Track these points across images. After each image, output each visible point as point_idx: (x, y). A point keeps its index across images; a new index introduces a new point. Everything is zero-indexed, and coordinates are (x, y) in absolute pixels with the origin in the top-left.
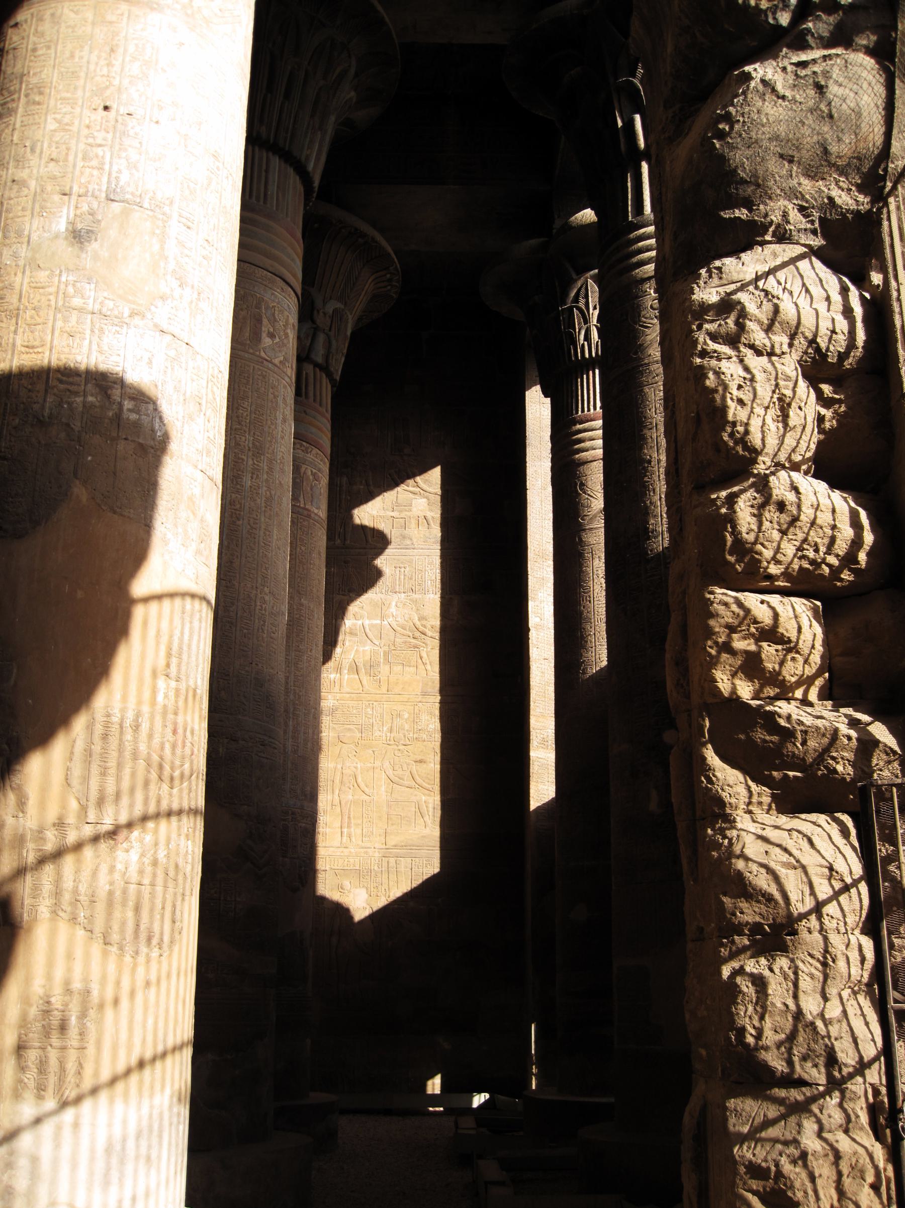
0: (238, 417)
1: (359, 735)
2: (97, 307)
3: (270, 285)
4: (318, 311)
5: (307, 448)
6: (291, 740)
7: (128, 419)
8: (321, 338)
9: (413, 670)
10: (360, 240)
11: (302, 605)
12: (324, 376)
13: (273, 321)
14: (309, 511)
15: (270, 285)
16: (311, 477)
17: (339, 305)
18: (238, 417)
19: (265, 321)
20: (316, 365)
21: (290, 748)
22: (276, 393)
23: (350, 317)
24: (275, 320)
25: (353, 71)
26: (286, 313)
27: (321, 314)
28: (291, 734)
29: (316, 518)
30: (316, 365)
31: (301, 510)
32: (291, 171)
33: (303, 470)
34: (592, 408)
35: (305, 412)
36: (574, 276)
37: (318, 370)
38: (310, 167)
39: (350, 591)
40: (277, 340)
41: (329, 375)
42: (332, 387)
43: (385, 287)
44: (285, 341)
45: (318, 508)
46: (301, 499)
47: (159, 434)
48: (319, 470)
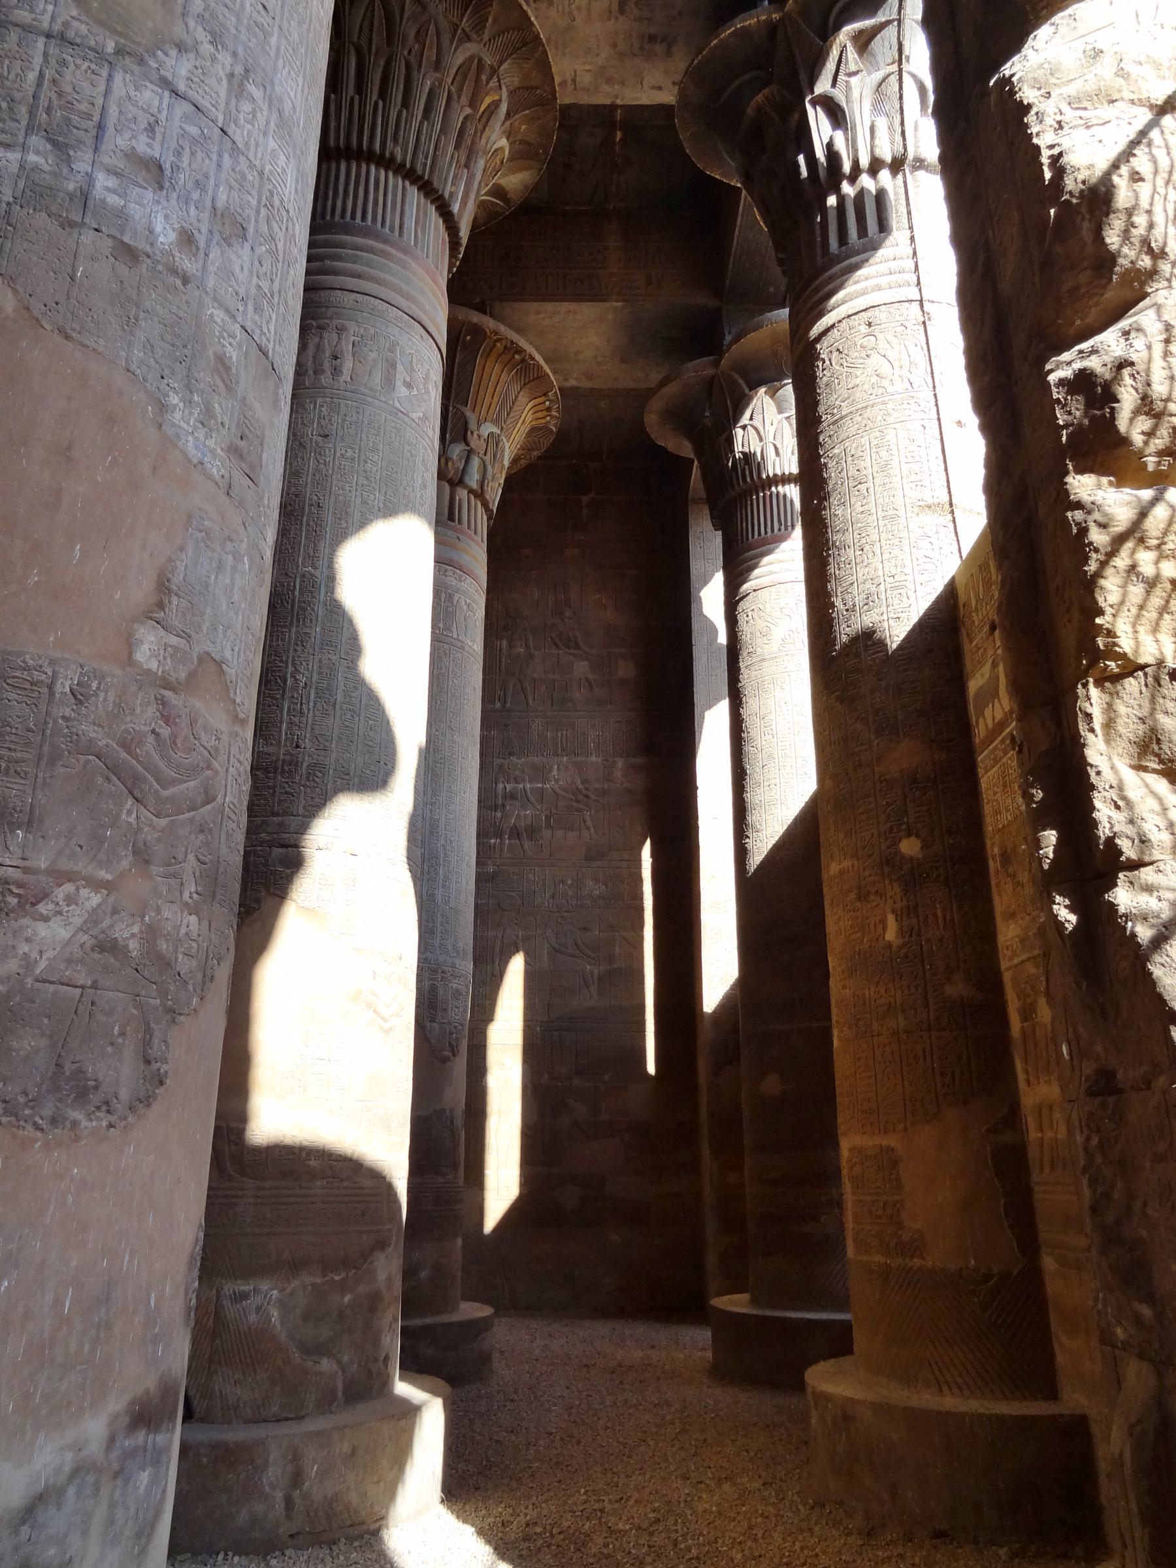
0: (365, 471)
1: (520, 902)
2: (57, 28)
3: (406, 329)
5: (460, 577)
7: (103, 201)
8: (476, 462)
9: (576, 834)
10: (517, 357)
11: (454, 742)
12: (479, 504)
13: (411, 370)
15: (406, 329)
17: (496, 430)
18: (365, 471)
19: (400, 367)
22: (414, 452)
23: (507, 445)
24: (413, 369)
25: (504, 108)
26: (426, 366)
30: (471, 491)
32: (432, 210)
33: (455, 599)
34: (769, 530)
36: (747, 391)
38: (455, 208)
39: (510, 755)
40: (415, 392)
41: (485, 505)
42: (489, 519)
43: (544, 418)
44: (425, 397)
45: (474, 641)
46: (454, 629)
47: (161, 239)
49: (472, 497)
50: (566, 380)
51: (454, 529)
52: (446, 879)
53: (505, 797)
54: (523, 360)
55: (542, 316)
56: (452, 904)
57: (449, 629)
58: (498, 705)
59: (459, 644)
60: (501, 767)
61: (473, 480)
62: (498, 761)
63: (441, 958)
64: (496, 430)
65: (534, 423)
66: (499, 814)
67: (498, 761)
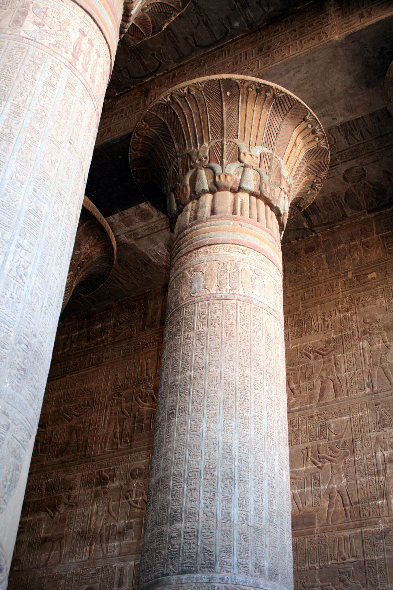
4: (245, 154)
6: (237, 508)
8: (251, 174)
10: (268, 94)
11: (247, 376)
16: (251, 273)
17: (266, 150)
20: (252, 194)
21: (236, 517)
23: (283, 162)
27: (248, 155)
28: (236, 501)
29: (261, 304)
30: (252, 194)
31: (240, 298)
33: (241, 266)
35: (240, 224)
37: (254, 199)
39: (383, 427)
40: (47, 28)
46: (240, 288)
48: (261, 268)
49: (269, 208)
50: (334, 119)
51: (235, 219)
52: (243, 498)
53: (385, 463)
54: (274, 97)
55: (292, 73)
56: (251, 521)
57: (236, 289)
58: (368, 390)
59: (246, 299)
60: (377, 438)
61: (251, 184)
62: (374, 434)
63: (240, 578)
64: (266, 150)
65: (307, 147)
66: (382, 478)
67: (374, 434)
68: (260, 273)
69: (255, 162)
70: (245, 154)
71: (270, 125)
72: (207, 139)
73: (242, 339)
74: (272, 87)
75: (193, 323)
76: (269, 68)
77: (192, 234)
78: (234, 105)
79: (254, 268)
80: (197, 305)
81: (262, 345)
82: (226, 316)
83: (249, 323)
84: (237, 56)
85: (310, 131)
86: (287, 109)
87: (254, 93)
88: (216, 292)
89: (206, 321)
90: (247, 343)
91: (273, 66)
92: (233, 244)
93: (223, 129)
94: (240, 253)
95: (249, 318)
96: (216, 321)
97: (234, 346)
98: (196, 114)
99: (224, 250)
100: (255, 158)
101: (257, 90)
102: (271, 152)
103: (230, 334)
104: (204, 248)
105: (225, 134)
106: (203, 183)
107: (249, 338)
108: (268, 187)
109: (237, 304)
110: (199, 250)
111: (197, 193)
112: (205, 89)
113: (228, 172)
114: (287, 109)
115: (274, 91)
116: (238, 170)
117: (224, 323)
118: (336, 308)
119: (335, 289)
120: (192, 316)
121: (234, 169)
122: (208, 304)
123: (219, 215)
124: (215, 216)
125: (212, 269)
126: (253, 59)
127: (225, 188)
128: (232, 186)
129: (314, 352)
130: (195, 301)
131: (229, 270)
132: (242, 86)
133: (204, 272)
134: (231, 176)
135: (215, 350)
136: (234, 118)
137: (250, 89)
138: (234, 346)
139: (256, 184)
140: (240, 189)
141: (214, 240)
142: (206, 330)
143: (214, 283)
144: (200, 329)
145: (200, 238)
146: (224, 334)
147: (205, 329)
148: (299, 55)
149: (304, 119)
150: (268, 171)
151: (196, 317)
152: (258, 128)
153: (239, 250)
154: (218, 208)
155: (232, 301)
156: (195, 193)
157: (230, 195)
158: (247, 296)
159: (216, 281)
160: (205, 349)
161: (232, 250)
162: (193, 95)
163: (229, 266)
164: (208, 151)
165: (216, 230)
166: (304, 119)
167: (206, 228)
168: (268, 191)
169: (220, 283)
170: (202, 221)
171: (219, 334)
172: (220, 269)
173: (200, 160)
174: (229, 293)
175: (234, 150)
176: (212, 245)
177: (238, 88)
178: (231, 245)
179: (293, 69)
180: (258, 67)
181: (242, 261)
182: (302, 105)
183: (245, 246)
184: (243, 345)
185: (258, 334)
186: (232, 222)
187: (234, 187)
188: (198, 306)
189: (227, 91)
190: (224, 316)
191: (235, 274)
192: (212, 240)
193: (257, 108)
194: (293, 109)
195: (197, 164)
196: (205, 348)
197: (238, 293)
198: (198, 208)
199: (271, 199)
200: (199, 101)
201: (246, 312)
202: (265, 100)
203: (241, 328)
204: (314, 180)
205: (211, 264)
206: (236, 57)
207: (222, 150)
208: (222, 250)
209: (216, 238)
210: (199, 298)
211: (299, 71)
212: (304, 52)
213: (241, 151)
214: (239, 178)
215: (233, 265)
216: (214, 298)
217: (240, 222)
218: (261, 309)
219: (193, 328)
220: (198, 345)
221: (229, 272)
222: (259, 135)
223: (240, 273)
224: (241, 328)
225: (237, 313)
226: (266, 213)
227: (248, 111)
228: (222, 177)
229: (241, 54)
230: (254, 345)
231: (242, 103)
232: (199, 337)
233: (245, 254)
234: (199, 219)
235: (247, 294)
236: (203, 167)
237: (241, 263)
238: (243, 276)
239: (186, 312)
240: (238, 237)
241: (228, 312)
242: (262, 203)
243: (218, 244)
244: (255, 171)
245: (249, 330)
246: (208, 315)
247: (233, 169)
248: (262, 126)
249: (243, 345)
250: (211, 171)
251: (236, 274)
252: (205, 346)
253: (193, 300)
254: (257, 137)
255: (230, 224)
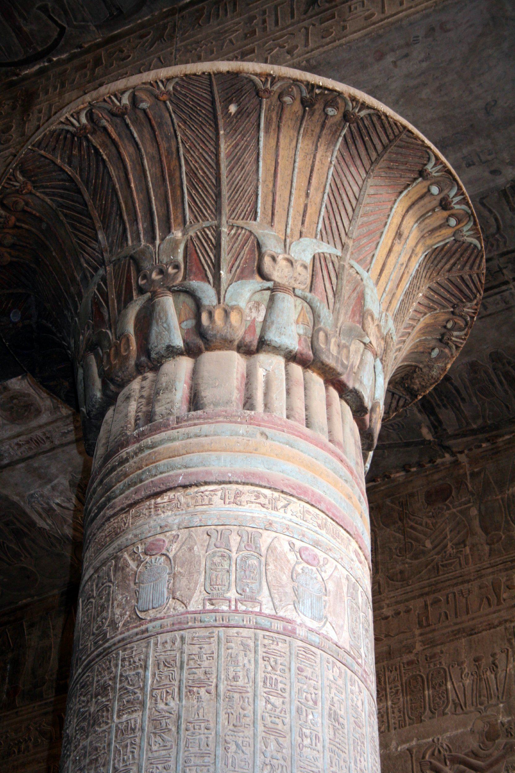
4: (274, 259)
10: (331, 111)
14: (289, 621)
16: (292, 557)
17: (326, 248)
20: (292, 357)
23: (368, 279)
29: (315, 639)
30: (292, 357)
33: (266, 539)
35: (263, 434)
46: (264, 596)
48: (316, 544)
49: (334, 393)
50: (495, 172)
51: (251, 421)
54: (346, 117)
55: (390, 58)
57: (253, 600)
59: (278, 625)
64: (326, 248)
65: (429, 242)
68: (315, 557)
69: (301, 278)
70: (274, 259)
71: (337, 188)
72: (180, 220)
73: (269, 731)
74: (340, 94)
75: (143, 689)
76: (334, 48)
77: (142, 459)
78: (247, 138)
79: (298, 544)
80: (152, 641)
81: (319, 747)
82: (227, 670)
83: (288, 688)
84: (254, 17)
85: (435, 203)
86: (379, 147)
87: (297, 107)
88: (201, 607)
89: (177, 683)
90: (281, 740)
91: (343, 41)
92: (244, 484)
93: (219, 195)
94: (263, 506)
95: (287, 675)
96: (201, 684)
97: (248, 751)
98: (151, 159)
99: (223, 498)
100: (300, 269)
101: (303, 102)
102: (339, 253)
103: (238, 718)
104: (171, 494)
105: (226, 209)
106: (168, 329)
107: (287, 728)
108: (333, 340)
109: (256, 639)
110: (159, 500)
111: (153, 355)
112: (175, 97)
113: (233, 303)
114: (379, 147)
115: (346, 104)
116: (257, 297)
117: (222, 687)
118: (507, 646)
119: (505, 596)
120: (140, 670)
121: (247, 295)
122: (182, 638)
123: (209, 409)
124: (200, 412)
125: (191, 549)
126: (292, 24)
127: (226, 343)
128: (243, 338)
129: (455, 760)
130: (147, 630)
131: (234, 549)
132: (266, 90)
133: (171, 555)
134: (240, 311)
135: (199, 761)
136: (247, 168)
137: (287, 99)
138: (248, 751)
139: (301, 332)
140: (263, 345)
141: (197, 474)
142: (176, 708)
143: (196, 584)
144: (161, 706)
145: (162, 469)
146: (223, 717)
147: (172, 704)
148: (408, 16)
149: (422, 174)
150: (331, 300)
151: (149, 674)
152: (307, 195)
153: (262, 500)
154: (208, 394)
155: (245, 632)
156: (147, 353)
157: (236, 361)
158: (282, 619)
159: (202, 579)
160: (173, 759)
161: (244, 498)
162: (144, 111)
163: (234, 540)
164: (181, 250)
165: (202, 449)
166: (422, 174)
167: (177, 443)
168: (334, 349)
169: (211, 583)
170: (166, 426)
171: (211, 717)
172: (212, 549)
173: (161, 272)
174: (236, 610)
175: (246, 249)
176: (191, 486)
177: (257, 94)
178: (240, 487)
179: (393, 50)
180: (306, 45)
181: (269, 526)
182: (417, 138)
183: (275, 489)
184: (273, 746)
185: (310, 717)
186: (242, 429)
187: (248, 339)
188: (156, 644)
189: (230, 102)
190: (222, 669)
191: (250, 562)
192: (191, 474)
193: (304, 145)
194: (393, 148)
195: (153, 281)
196: (173, 755)
197: (257, 609)
198: (158, 393)
199: (339, 369)
200: (160, 125)
201: (280, 660)
202: (323, 126)
203: (268, 701)
204: (448, 321)
205: (190, 536)
206: (252, 19)
207: (218, 247)
208: (216, 499)
209: (201, 469)
210: (158, 623)
211: (407, 55)
212: (419, 8)
213: (264, 250)
214: (261, 319)
215: (245, 538)
216: (197, 624)
217: (263, 429)
218: (319, 652)
219: (143, 704)
220: (154, 748)
221: (234, 555)
222: (309, 211)
223: (263, 559)
224: (268, 701)
225: (256, 662)
226: (329, 405)
227: (281, 152)
228: (218, 315)
229: (264, 12)
230: (301, 746)
231: (267, 132)
232: (159, 727)
233: (275, 508)
234: (158, 419)
235: (281, 613)
236: (169, 289)
237: (265, 533)
238: (271, 567)
239: (123, 660)
240: (257, 466)
241: (233, 659)
242: (317, 381)
243: (206, 483)
244: (299, 301)
245: (286, 707)
246: (182, 668)
247: (244, 294)
248: (317, 190)
249: (273, 746)
250: (189, 301)
251: (254, 562)
252: (174, 750)
253: (143, 627)
254: (304, 216)
255: (237, 434)
